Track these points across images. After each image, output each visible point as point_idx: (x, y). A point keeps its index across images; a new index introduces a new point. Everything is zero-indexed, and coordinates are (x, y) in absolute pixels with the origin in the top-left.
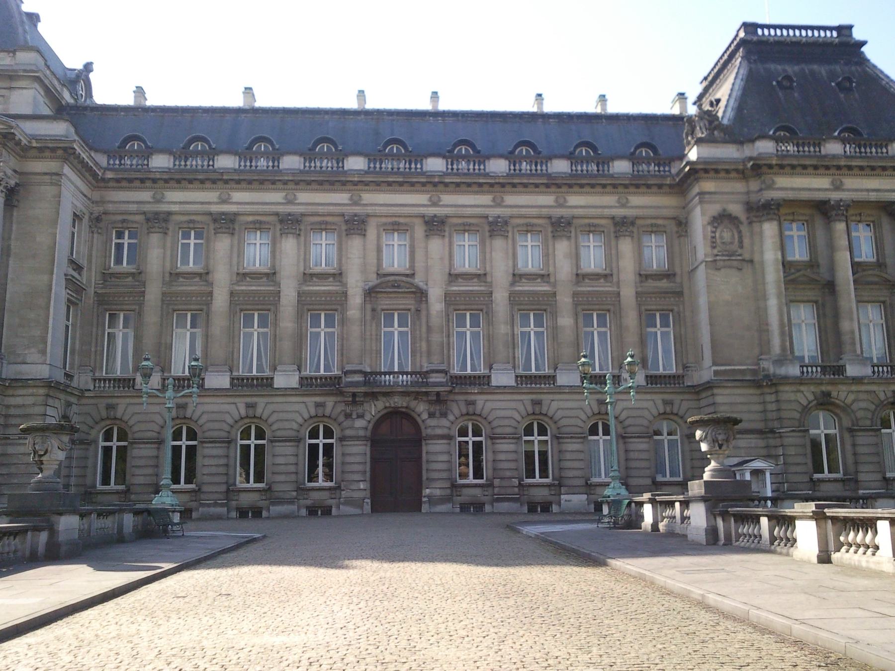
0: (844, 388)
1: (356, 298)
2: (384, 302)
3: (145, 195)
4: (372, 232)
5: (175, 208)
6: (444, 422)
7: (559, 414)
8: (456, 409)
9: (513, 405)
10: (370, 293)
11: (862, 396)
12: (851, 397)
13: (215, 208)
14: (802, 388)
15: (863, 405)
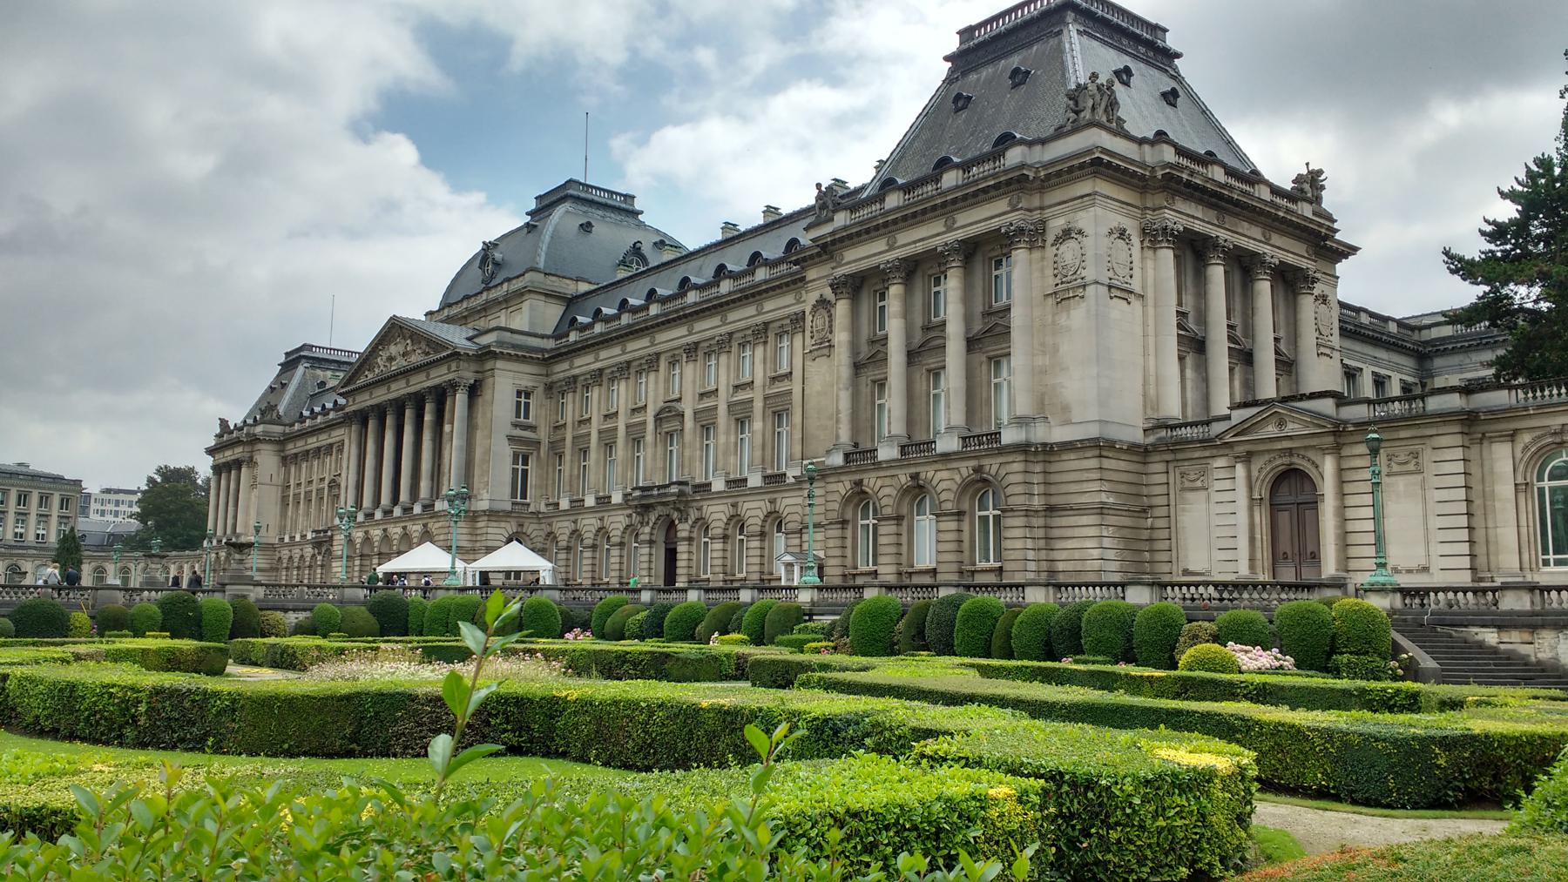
0: (874, 474)
1: (650, 426)
2: (666, 427)
3: (565, 366)
4: (663, 365)
5: (577, 371)
6: (686, 526)
7: (749, 513)
8: (693, 515)
9: (722, 508)
10: (658, 419)
11: (888, 481)
12: (879, 483)
13: (593, 367)
14: (843, 478)
15: (887, 491)
